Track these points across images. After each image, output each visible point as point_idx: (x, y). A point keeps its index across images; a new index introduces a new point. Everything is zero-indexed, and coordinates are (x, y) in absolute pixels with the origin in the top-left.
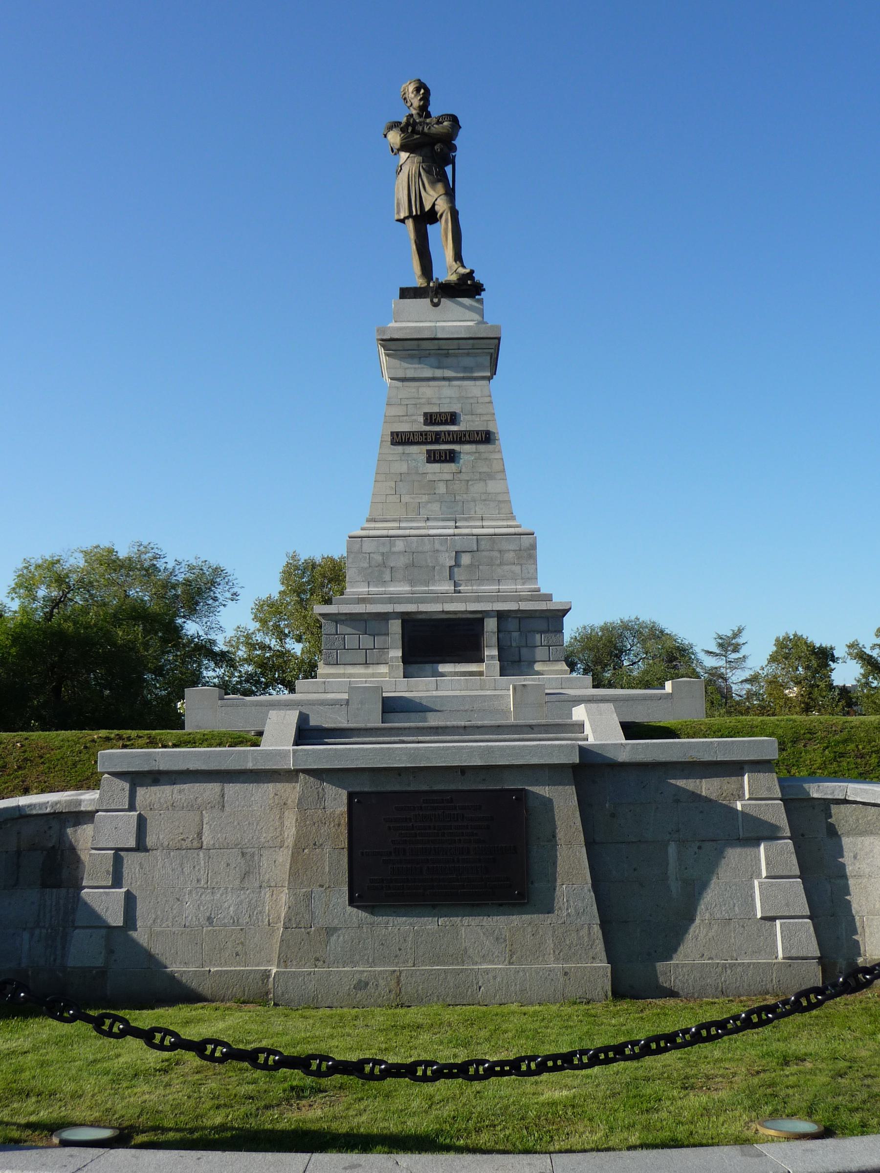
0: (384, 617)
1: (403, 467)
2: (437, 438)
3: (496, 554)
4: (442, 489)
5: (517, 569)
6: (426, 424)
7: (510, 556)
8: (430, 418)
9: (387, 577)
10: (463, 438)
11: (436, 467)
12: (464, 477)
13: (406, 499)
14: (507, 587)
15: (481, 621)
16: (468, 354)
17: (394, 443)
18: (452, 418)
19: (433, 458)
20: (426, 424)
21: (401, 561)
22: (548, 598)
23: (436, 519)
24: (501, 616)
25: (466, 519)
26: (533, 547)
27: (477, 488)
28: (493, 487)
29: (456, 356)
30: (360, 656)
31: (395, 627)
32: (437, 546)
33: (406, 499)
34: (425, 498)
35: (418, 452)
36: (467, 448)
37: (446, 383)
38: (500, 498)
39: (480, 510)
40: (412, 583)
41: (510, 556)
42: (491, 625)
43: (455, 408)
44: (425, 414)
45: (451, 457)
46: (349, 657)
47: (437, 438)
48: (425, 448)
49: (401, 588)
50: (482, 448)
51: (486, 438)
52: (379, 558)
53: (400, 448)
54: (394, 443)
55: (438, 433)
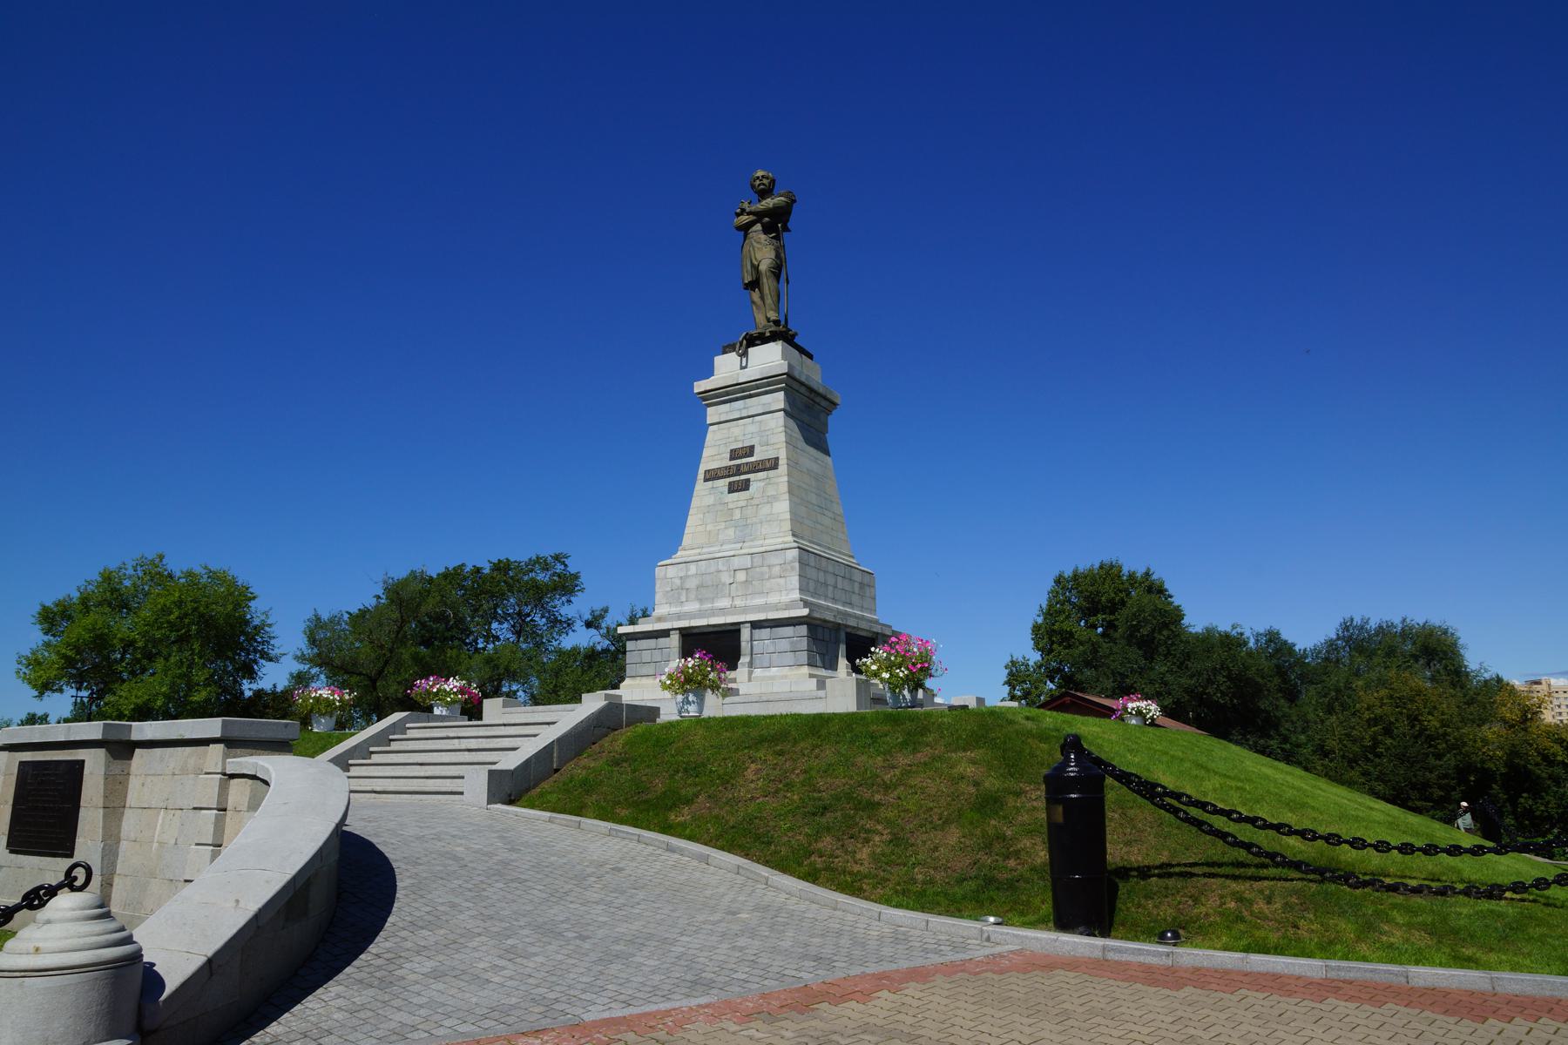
0: (665, 633)
1: (710, 500)
2: (738, 470)
3: (765, 569)
5: (782, 581)
7: (776, 570)
8: (734, 454)
12: (755, 502)
14: (773, 599)
18: (750, 451)
19: (733, 489)
21: (692, 583)
23: (730, 542)
24: (756, 625)
31: (674, 641)
34: (723, 525)
35: (723, 484)
36: (761, 475)
40: (701, 601)
42: (745, 633)
45: (745, 486)
47: (738, 470)
48: (728, 480)
49: (693, 606)
50: (772, 473)
52: (678, 582)
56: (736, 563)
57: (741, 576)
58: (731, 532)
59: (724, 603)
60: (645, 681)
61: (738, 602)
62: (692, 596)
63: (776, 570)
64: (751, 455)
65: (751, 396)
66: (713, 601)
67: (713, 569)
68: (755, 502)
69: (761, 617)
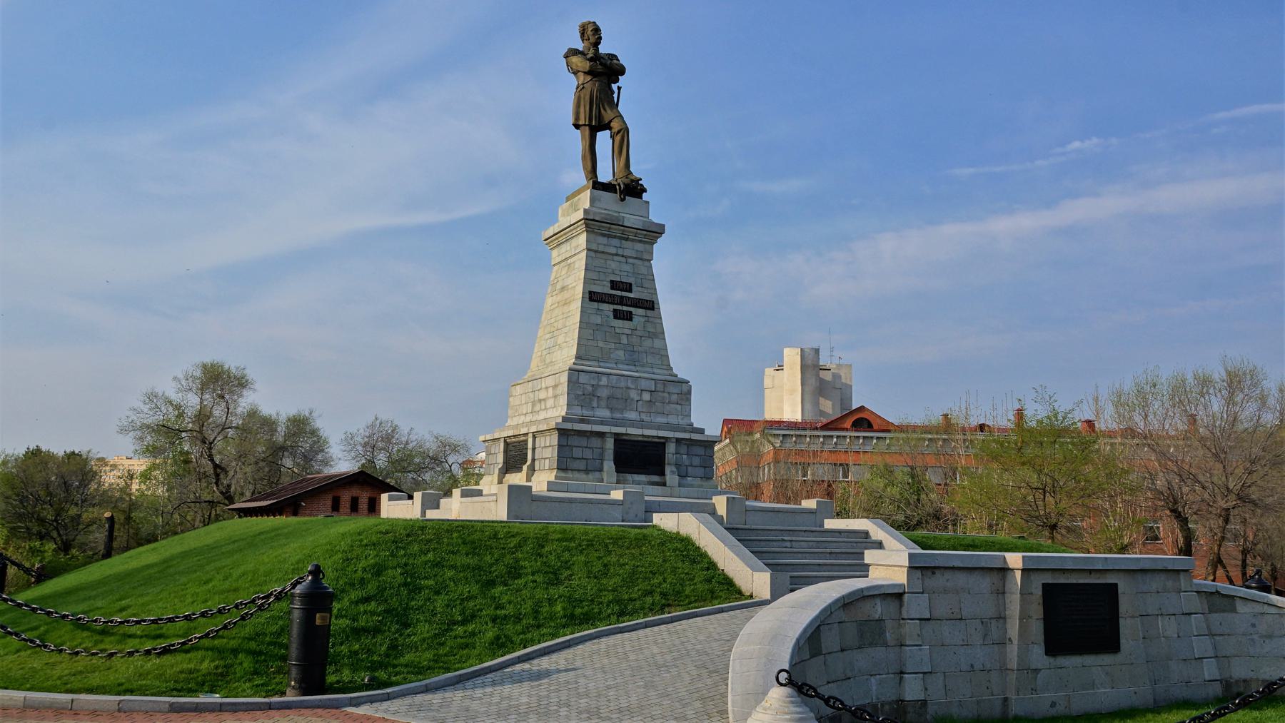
0: (601, 435)
1: (598, 320)
2: (622, 301)
4: (624, 340)
5: (679, 407)
6: (612, 288)
8: (614, 285)
9: (595, 404)
10: (638, 303)
11: (619, 323)
12: (638, 333)
13: (601, 344)
14: (673, 420)
15: (663, 445)
16: (640, 241)
17: (591, 299)
18: (628, 288)
19: (617, 315)
20: (612, 288)
21: (604, 393)
22: (701, 431)
24: (678, 441)
25: (643, 366)
26: (689, 392)
27: (647, 343)
28: (657, 343)
29: (633, 240)
30: (582, 465)
31: (610, 444)
32: (630, 385)
33: (601, 344)
34: (613, 346)
36: (641, 311)
37: (623, 260)
38: (662, 352)
39: (650, 359)
40: (612, 409)
41: (675, 397)
42: (671, 448)
43: (631, 280)
44: (612, 282)
45: (628, 317)
46: (576, 465)
47: (622, 301)
48: (612, 307)
49: (604, 413)
50: (649, 313)
51: (650, 305)
52: (590, 388)
53: (595, 305)
54: (591, 299)
55: (622, 297)
56: (644, 384)
57: (646, 396)
58: (621, 353)
59: (632, 415)
60: (577, 475)
61: (644, 416)
62: (603, 403)
63: (675, 397)
64: (630, 291)
65: (627, 239)
66: (621, 411)
67: (623, 384)
68: (638, 333)
69: (686, 436)
